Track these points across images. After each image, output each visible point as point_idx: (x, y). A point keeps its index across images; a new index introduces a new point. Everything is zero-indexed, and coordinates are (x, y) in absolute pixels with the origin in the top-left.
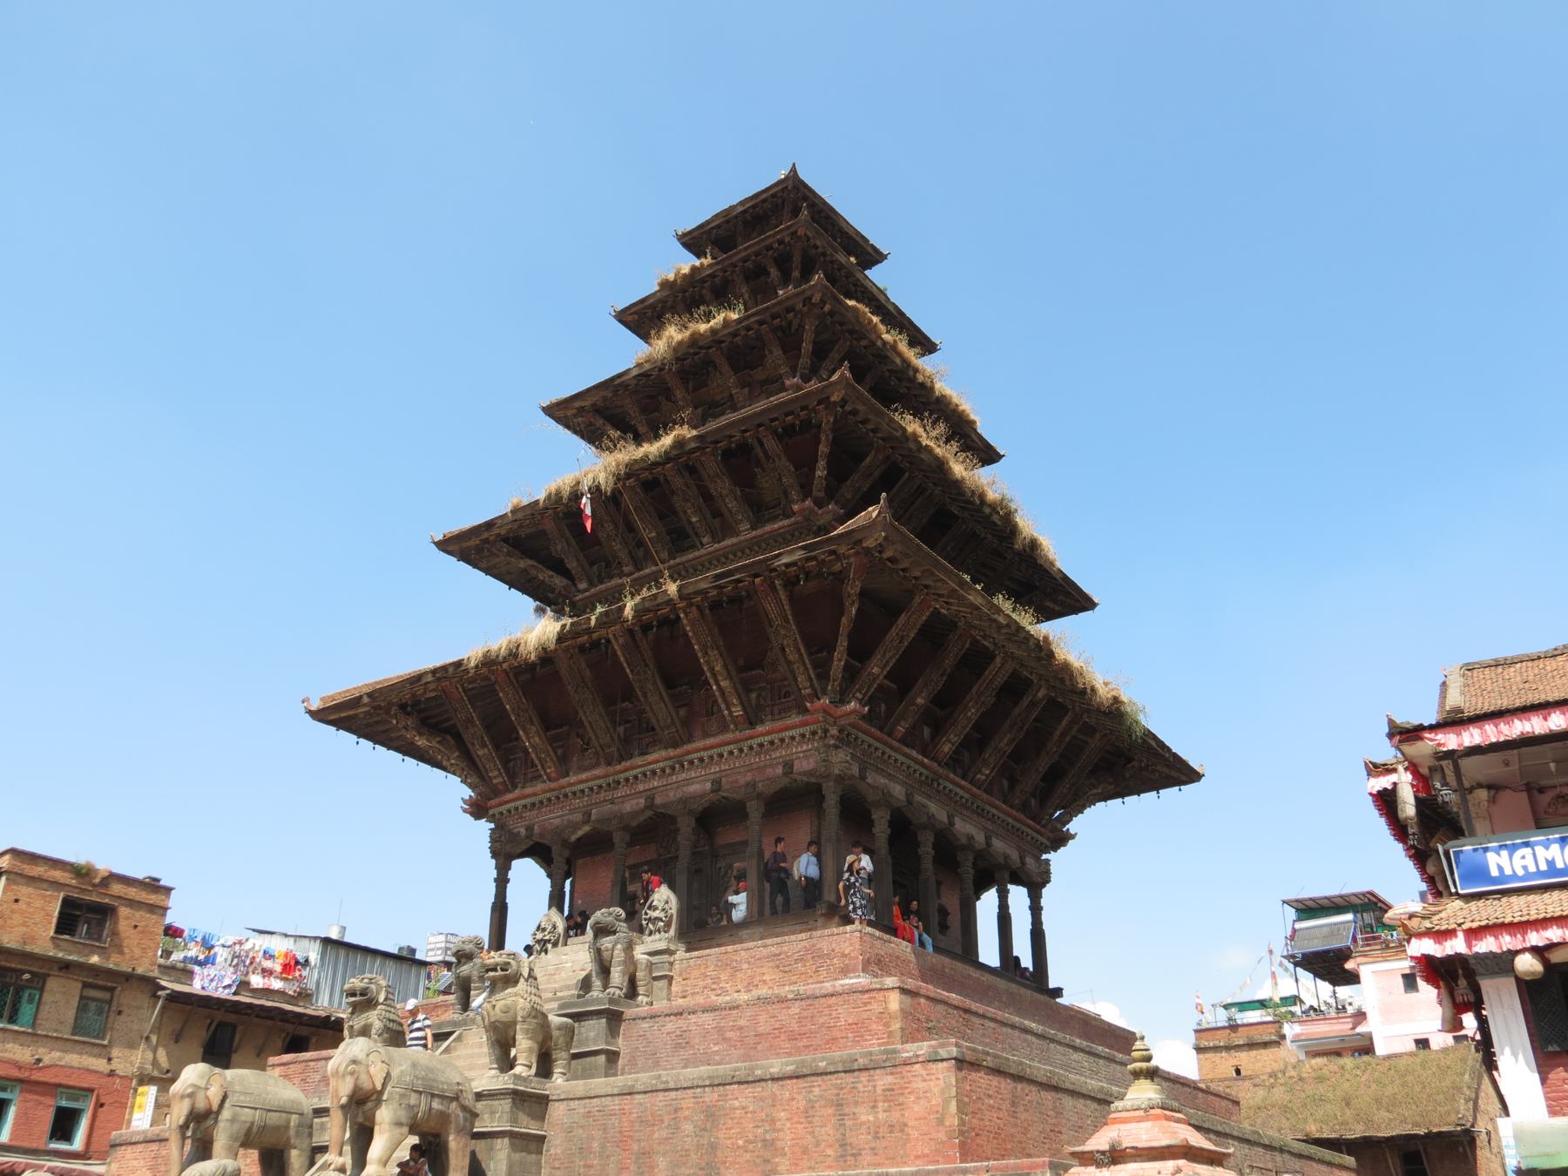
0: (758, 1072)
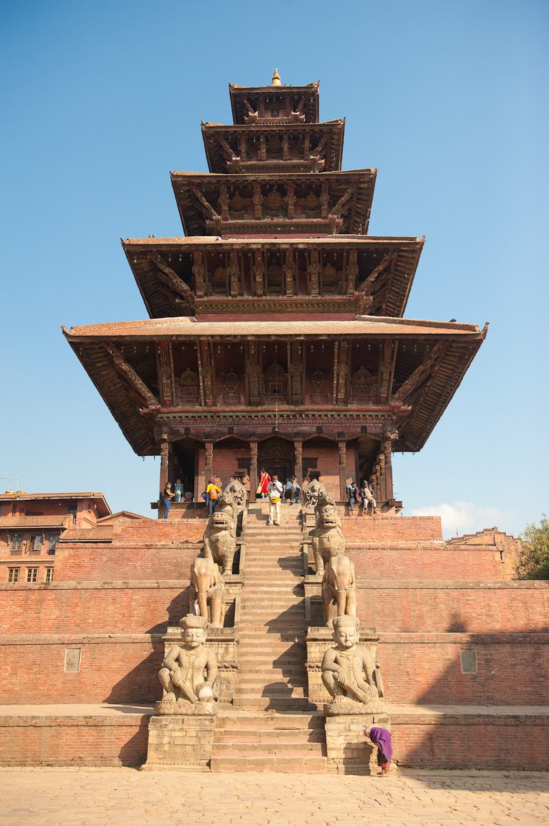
0: (481, 585)
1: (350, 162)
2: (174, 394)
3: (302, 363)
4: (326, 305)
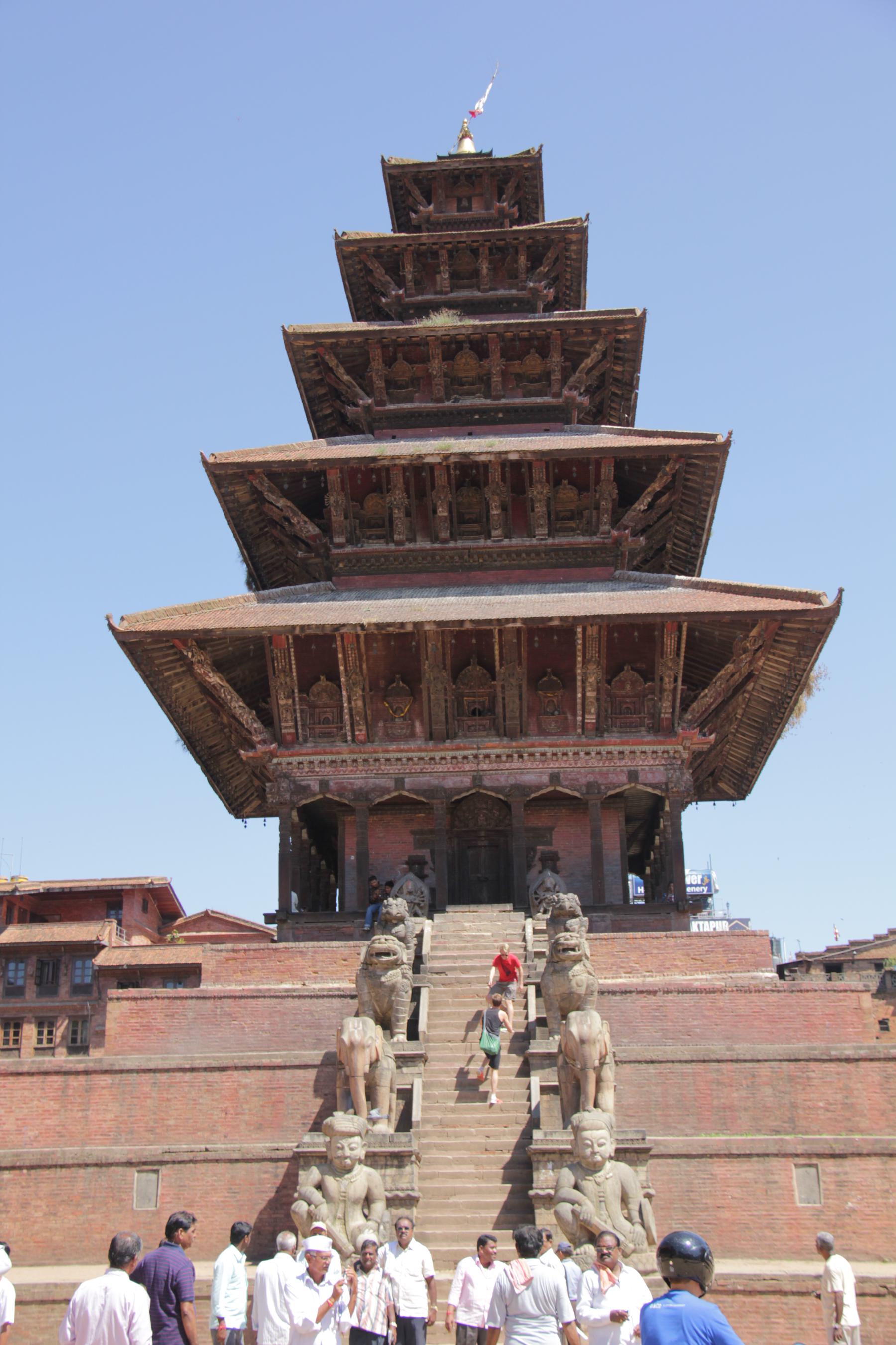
0: (833, 1053)
1: (602, 294)
2: (299, 723)
3: (520, 663)
4: (561, 553)
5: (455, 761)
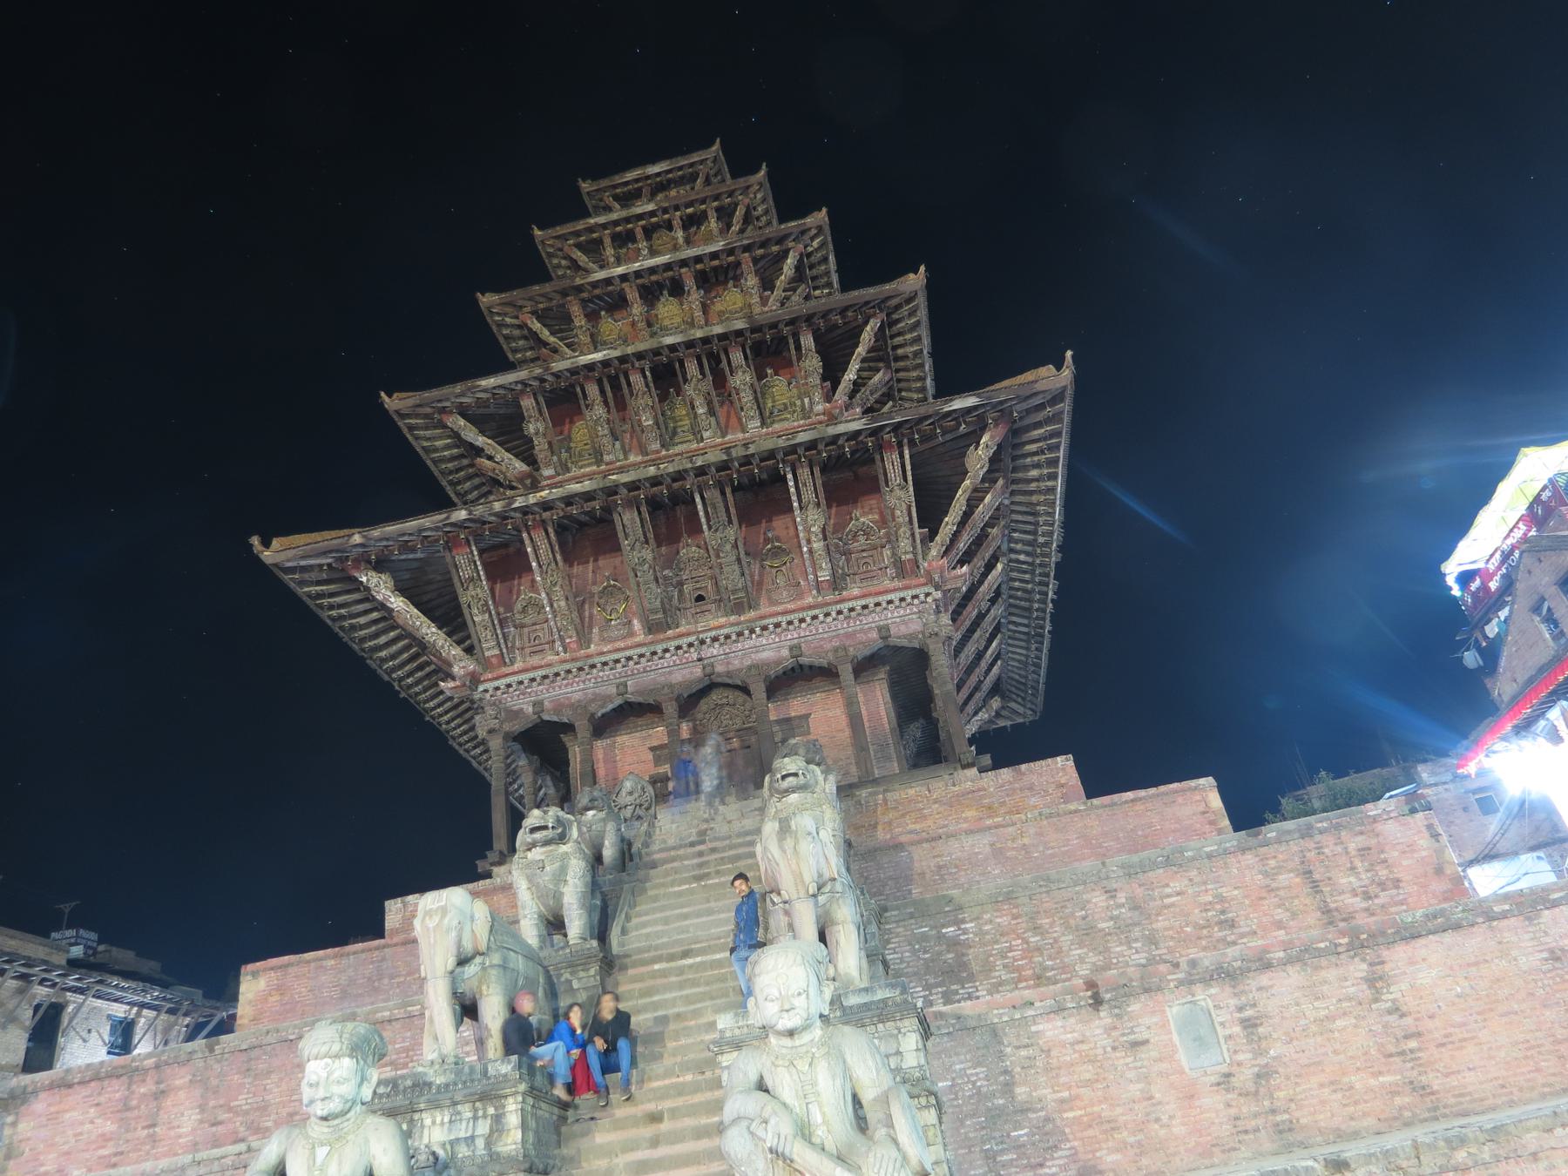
3: (730, 522)
5: (680, 652)
